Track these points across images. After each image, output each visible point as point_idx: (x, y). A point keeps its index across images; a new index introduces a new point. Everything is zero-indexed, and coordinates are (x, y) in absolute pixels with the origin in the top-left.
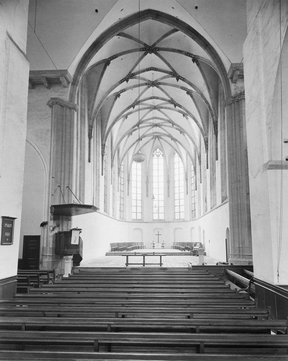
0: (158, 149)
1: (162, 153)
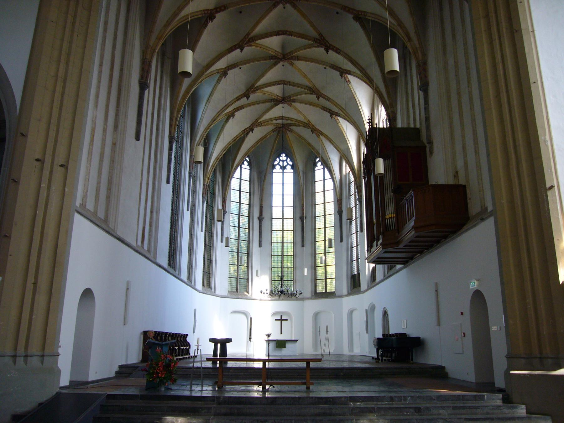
0: (283, 155)
1: (291, 163)
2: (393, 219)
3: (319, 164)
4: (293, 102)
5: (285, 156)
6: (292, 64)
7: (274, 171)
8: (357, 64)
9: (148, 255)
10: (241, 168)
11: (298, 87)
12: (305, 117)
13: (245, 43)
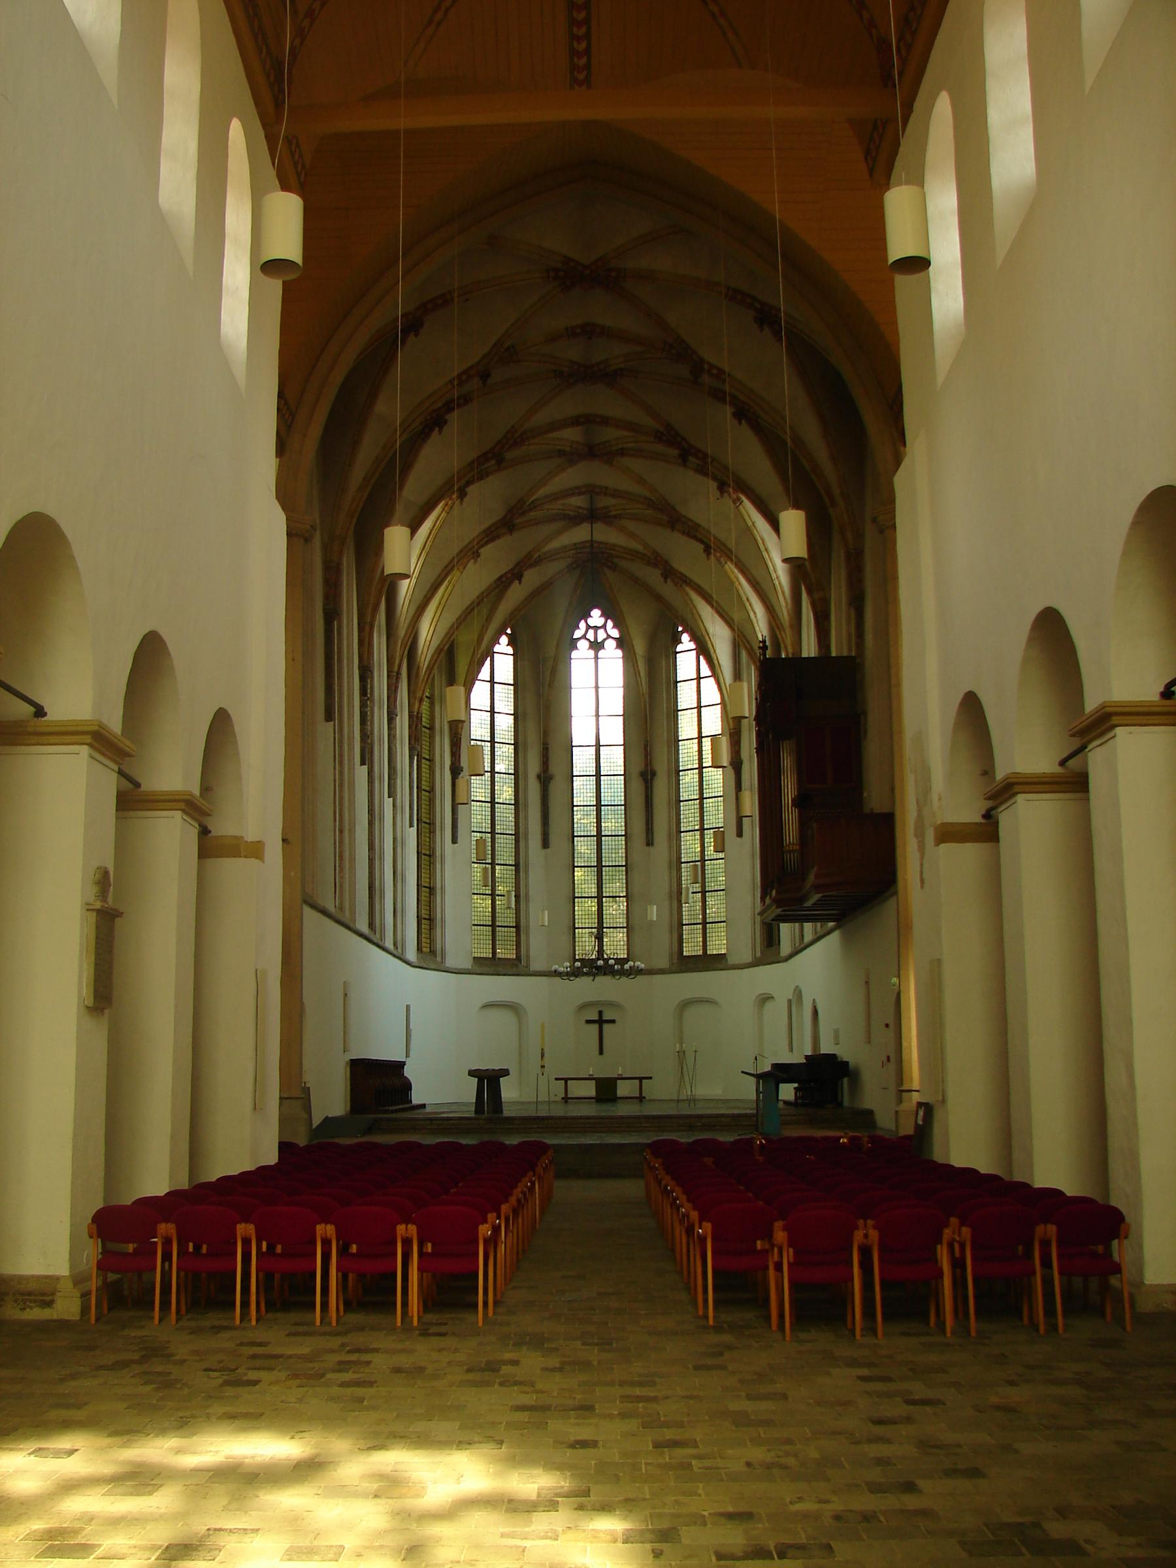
0: (596, 613)
1: (615, 633)
7: (574, 654)
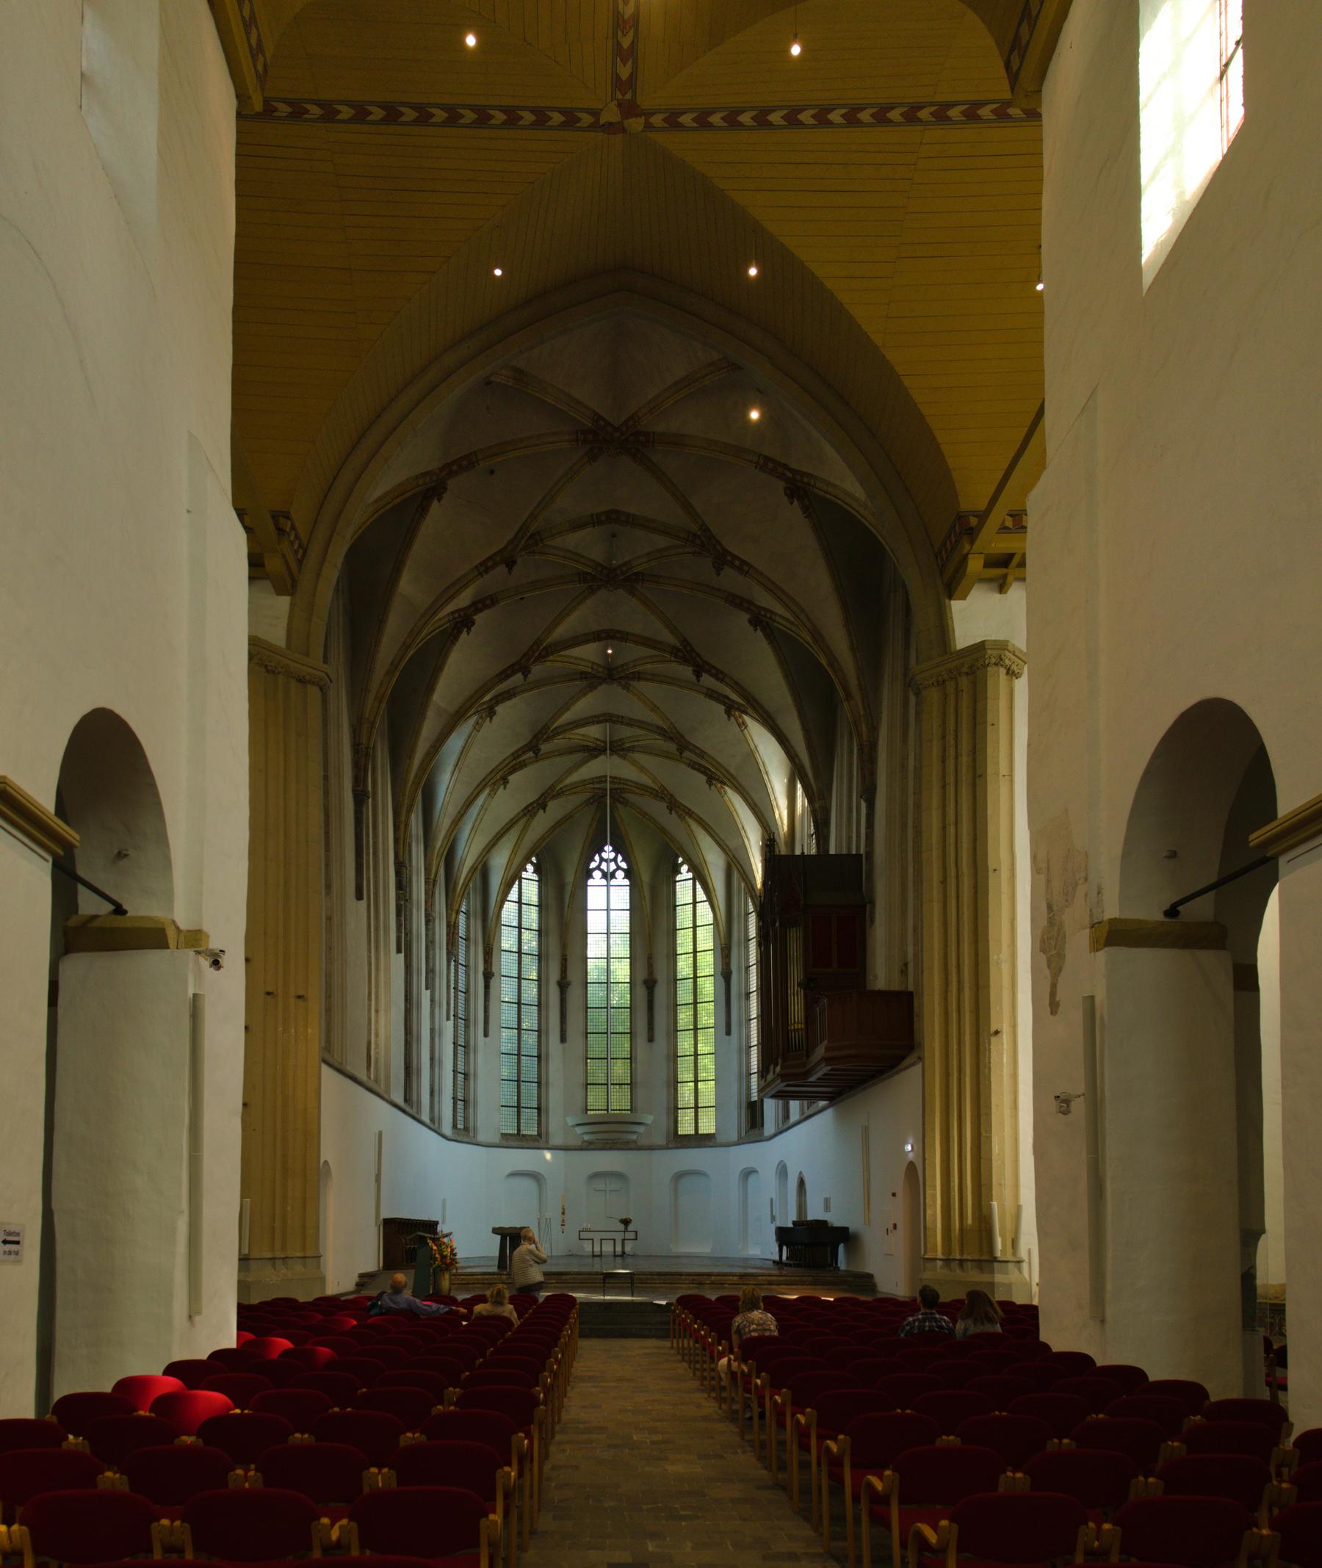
0: (608, 848)
1: (624, 865)
2: (800, 1032)
3: (684, 868)
4: (633, 679)
5: (612, 851)
6: (626, 687)
7: (590, 882)
8: (758, 703)
9: (375, 1087)
10: (521, 879)
11: (640, 727)
12: (654, 779)
13: (532, 660)
